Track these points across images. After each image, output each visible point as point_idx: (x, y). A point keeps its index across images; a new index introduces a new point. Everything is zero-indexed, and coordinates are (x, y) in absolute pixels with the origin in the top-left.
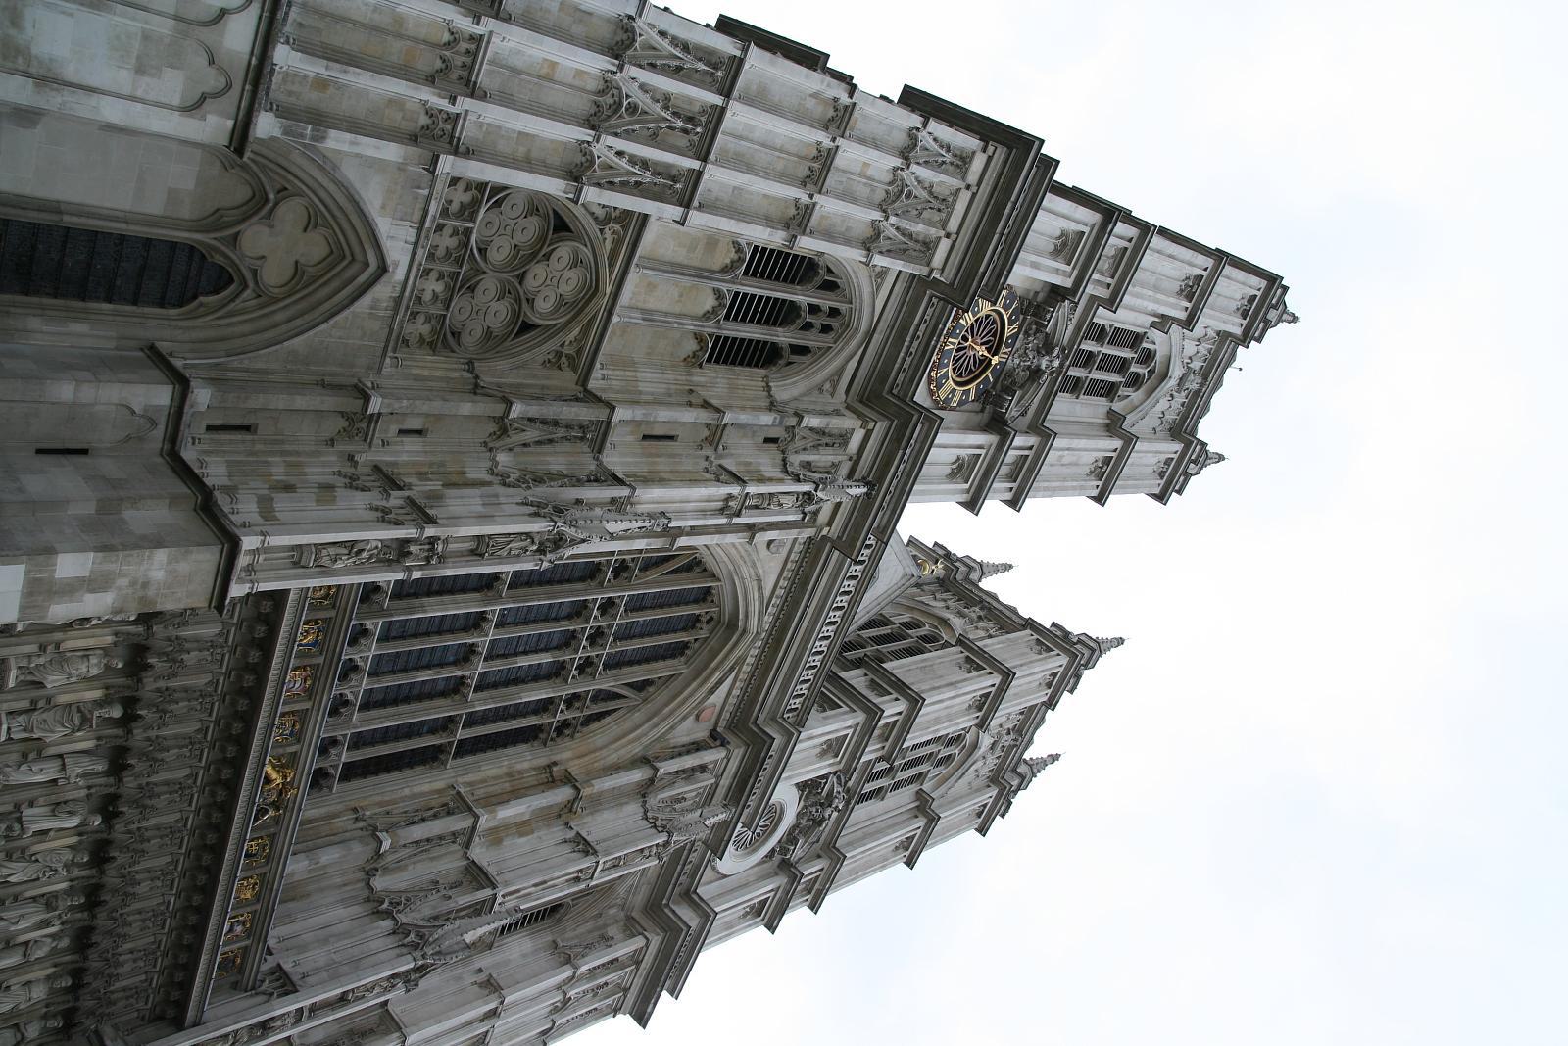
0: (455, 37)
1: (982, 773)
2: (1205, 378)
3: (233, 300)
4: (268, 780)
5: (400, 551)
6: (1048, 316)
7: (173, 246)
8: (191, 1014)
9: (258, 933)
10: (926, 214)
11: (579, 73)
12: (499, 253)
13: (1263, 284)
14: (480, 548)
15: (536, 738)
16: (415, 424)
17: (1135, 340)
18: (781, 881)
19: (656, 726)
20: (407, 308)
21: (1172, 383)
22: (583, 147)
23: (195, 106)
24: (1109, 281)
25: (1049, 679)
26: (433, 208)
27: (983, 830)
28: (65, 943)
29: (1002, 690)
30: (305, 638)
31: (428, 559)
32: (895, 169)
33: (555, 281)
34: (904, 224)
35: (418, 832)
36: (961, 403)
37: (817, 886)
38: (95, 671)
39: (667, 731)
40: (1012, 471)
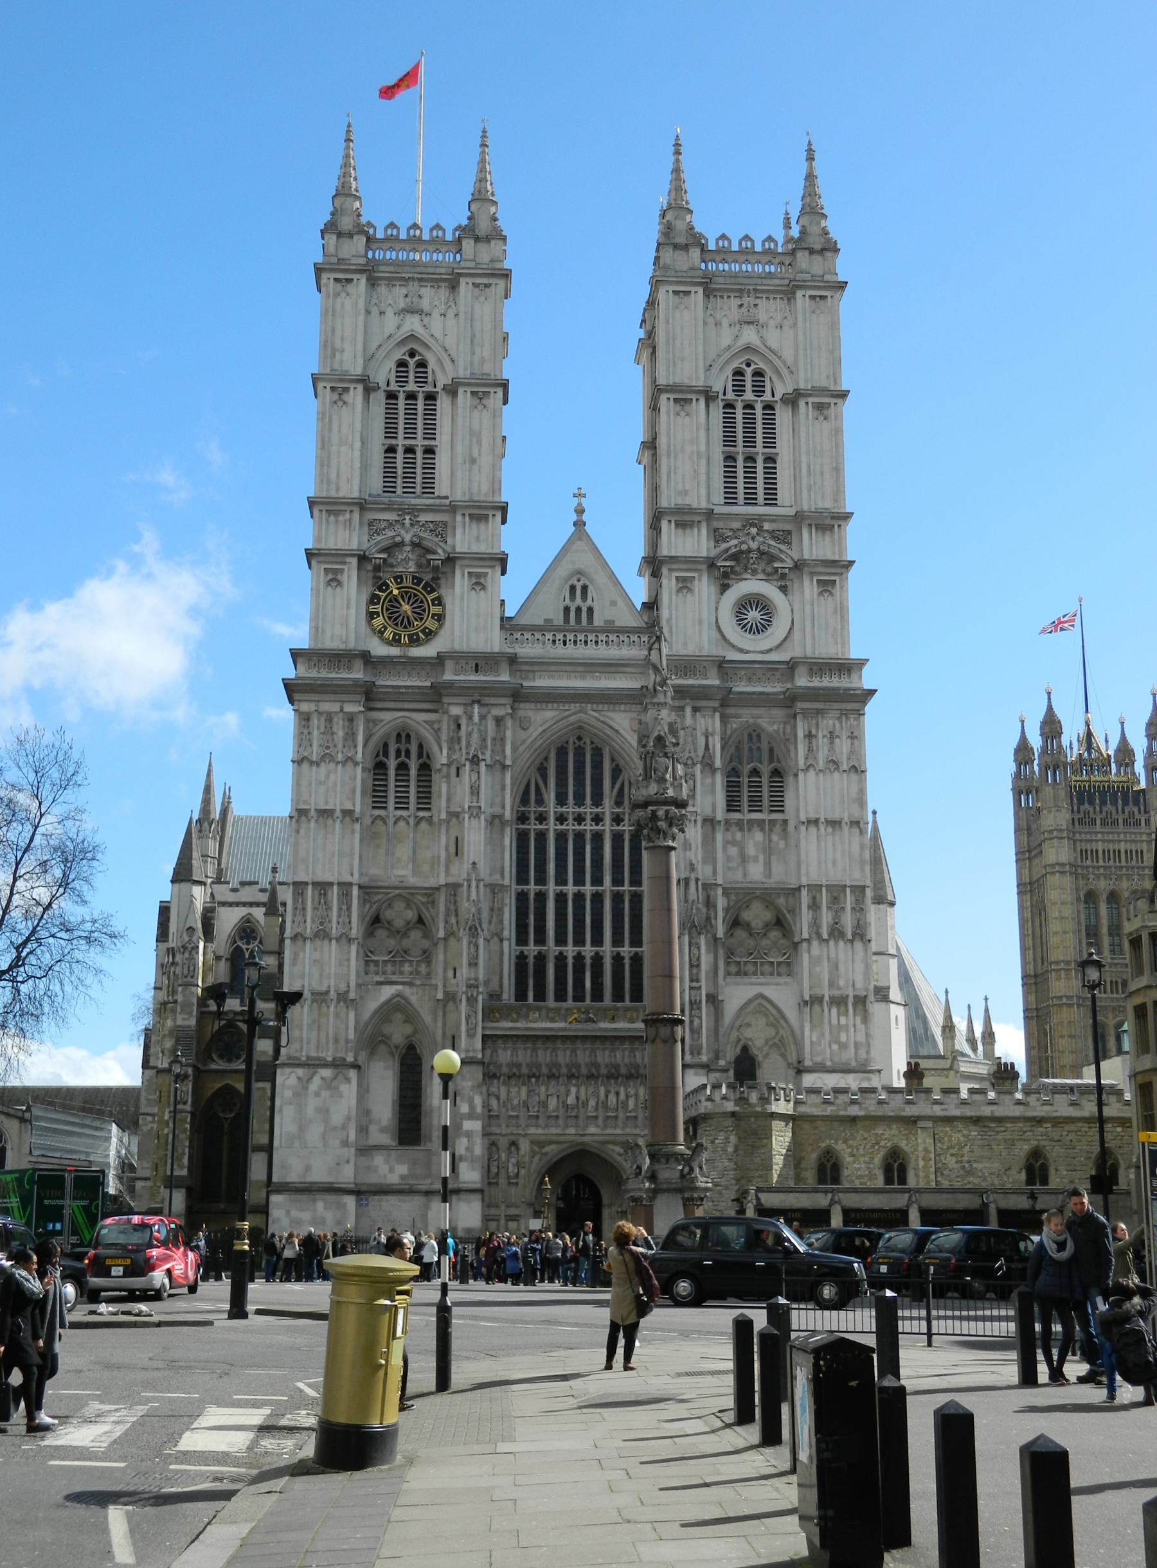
0: (313, 1001)
1: (779, 318)
5: (472, 1001)
7: (402, 1065)
10: (335, 730)
11: (315, 950)
13: (325, 276)
14: (473, 964)
16: (450, 973)
17: (391, 396)
22: (338, 940)
23: (348, 1080)
24: (348, 516)
26: (378, 978)
27: (842, 286)
28: (631, 1084)
29: (671, 389)
32: (318, 765)
34: (340, 746)
36: (440, 604)
37: (828, 521)
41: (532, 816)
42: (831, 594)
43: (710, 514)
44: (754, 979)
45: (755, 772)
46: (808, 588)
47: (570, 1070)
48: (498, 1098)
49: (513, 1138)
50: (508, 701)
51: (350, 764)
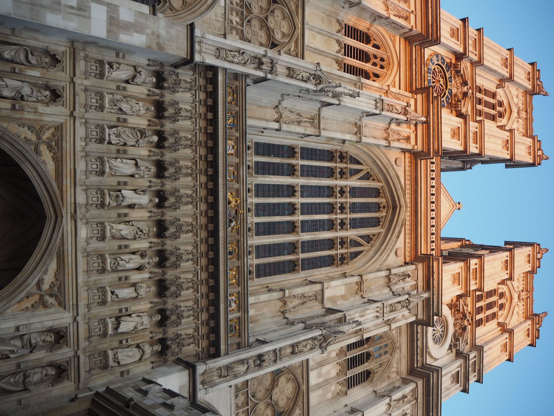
2: (526, 112)
3: (163, 7)
4: (230, 203)
5: (259, 63)
6: (459, 66)
8: (223, 347)
9: (243, 308)
12: (256, 11)
14: (291, 73)
15: (333, 264)
17: (494, 95)
18: (460, 362)
19: (381, 255)
20: (228, 24)
21: (515, 114)
24: (475, 52)
25: (527, 259)
28: (153, 289)
30: (229, 120)
31: (272, 68)
33: (279, 25)
35: (299, 291)
38: (143, 111)
39: (387, 257)
40: (474, 140)
41: (343, 165)
42: (452, 382)
43: (480, 289)
44: (234, 407)
45: (368, 356)
46: (456, 366)
47: (173, 193)
48: (127, 82)
49: (67, 94)
50: (419, 148)
51: (385, 8)
